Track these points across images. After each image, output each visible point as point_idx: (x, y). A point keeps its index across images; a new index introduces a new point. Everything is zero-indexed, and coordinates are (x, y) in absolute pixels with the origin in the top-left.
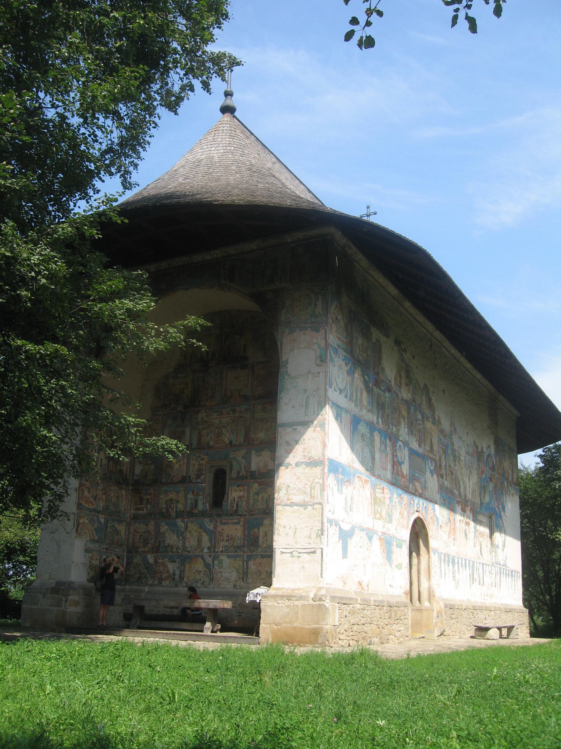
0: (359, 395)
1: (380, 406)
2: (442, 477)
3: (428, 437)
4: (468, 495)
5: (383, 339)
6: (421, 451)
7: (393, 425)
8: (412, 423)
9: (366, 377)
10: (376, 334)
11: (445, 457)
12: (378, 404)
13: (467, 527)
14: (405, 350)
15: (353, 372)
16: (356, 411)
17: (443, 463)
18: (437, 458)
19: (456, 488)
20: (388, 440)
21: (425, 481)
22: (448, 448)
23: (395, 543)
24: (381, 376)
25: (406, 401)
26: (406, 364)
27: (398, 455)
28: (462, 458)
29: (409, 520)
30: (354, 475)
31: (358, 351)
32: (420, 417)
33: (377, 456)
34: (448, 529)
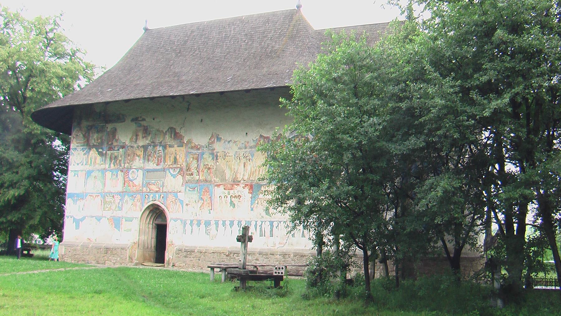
0: (93, 160)
1: (114, 159)
2: (192, 174)
3: (170, 157)
4: (238, 176)
5: (118, 125)
6: (159, 167)
7: (124, 163)
8: (150, 155)
9: (100, 150)
10: (110, 127)
11: (198, 161)
12: (111, 158)
13: (233, 199)
14: (144, 120)
15: (89, 153)
16: (91, 168)
17: (194, 164)
18: (184, 164)
19: (217, 177)
20: (119, 173)
21: (163, 183)
22: (203, 154)
23: (124, 220)
24: (115, 144)
25: (143, 146)
26: (144, 126)
27: (130, 177)
28: (232, 153)
29: (143, 206)
30: (86, 196)
31: (93, 141)
32: (161, 149)
33: (108, 182)
34: (200, 204)
